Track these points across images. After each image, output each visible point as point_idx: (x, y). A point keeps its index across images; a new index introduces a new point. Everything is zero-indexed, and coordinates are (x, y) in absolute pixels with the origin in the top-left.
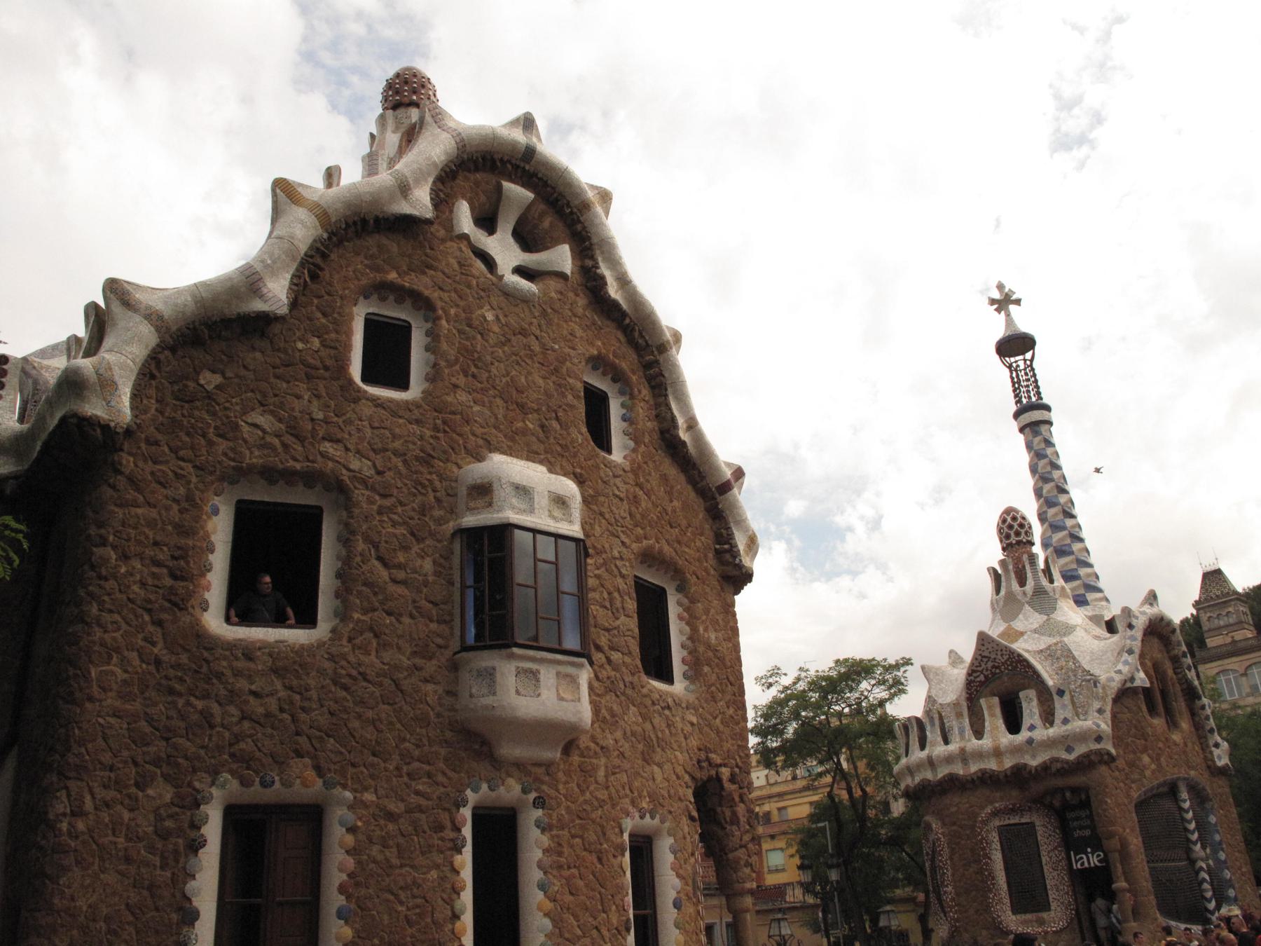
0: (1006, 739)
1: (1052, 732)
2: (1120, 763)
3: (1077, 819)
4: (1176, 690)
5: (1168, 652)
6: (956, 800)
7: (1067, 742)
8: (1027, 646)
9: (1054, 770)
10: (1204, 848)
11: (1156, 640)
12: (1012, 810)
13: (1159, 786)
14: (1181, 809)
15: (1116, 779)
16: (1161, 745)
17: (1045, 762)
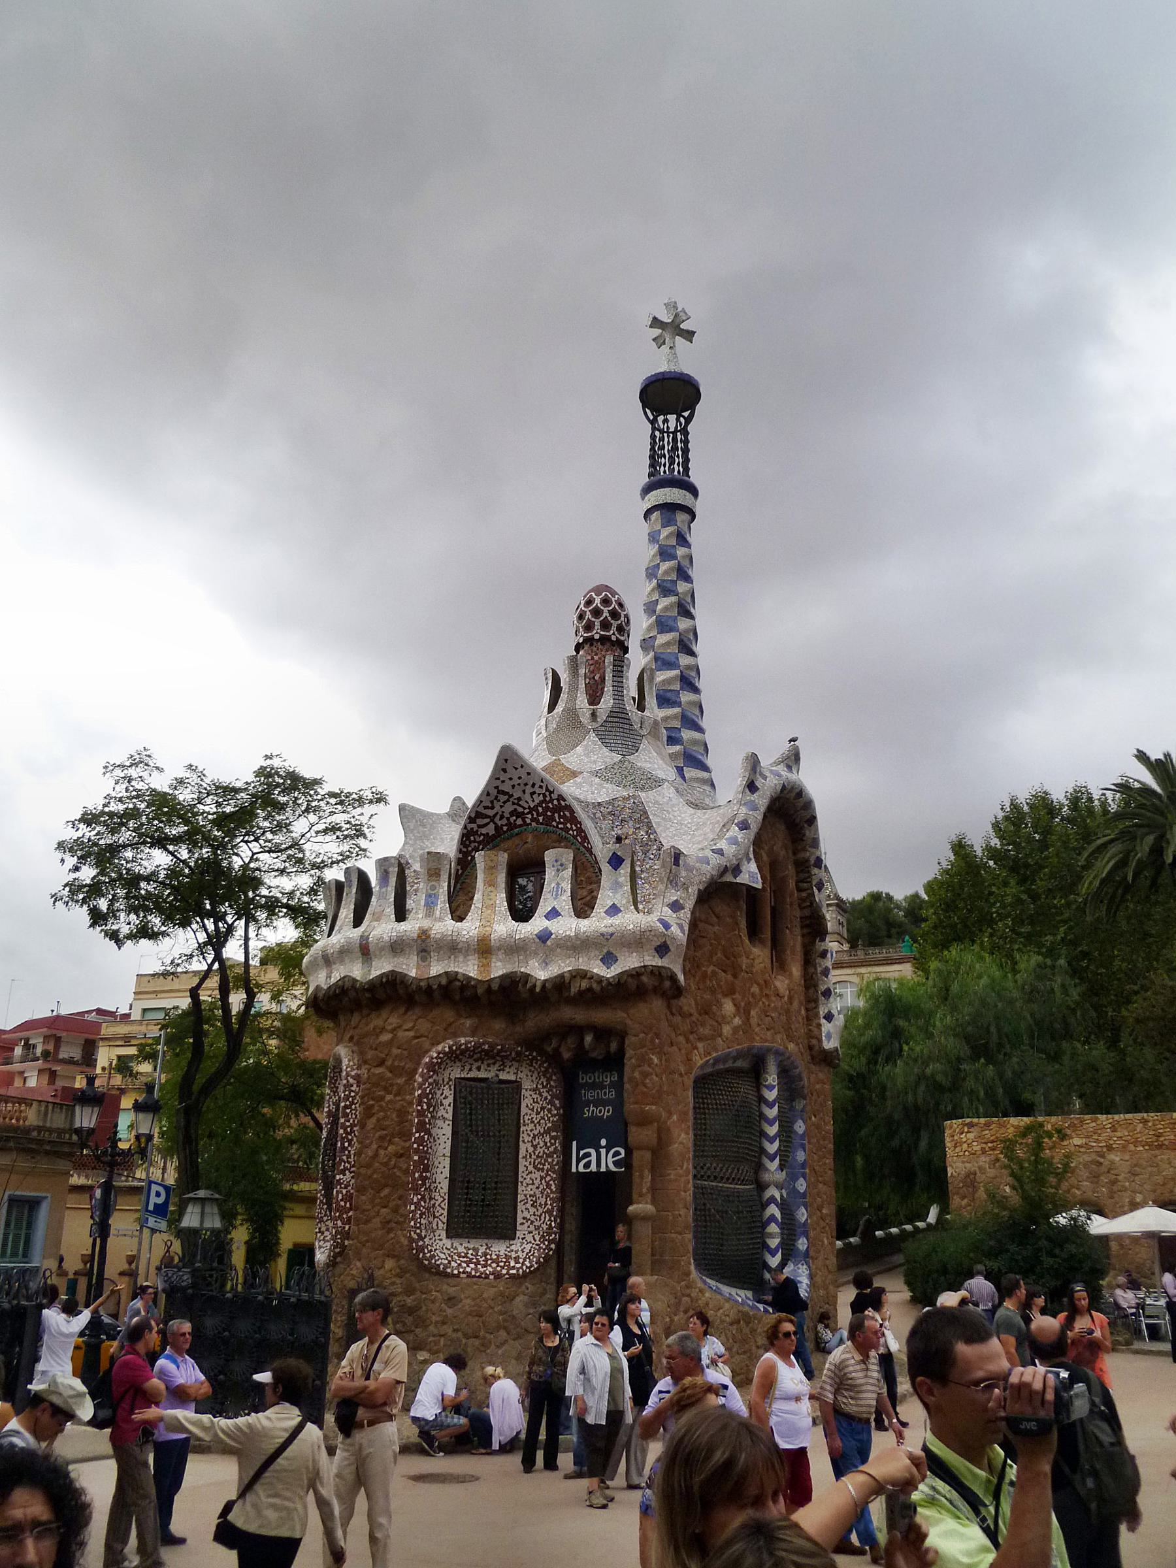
0: (504, 927)
1: (584, 926)
2: (687, 1003)
3: (594, 1086)
4: (794, 914)
5: (794, 854)
6: (394, 1020)
7: (607, 946)
8: (577, 792)
9: (574, 990)
10: (781, 1167)
11: (783, 827)
12: (487, 1053)
13: (740, 1055)
14: (761, 1099)
15: (674, 1028)
16: (755, 989)
17: (562, 976)
